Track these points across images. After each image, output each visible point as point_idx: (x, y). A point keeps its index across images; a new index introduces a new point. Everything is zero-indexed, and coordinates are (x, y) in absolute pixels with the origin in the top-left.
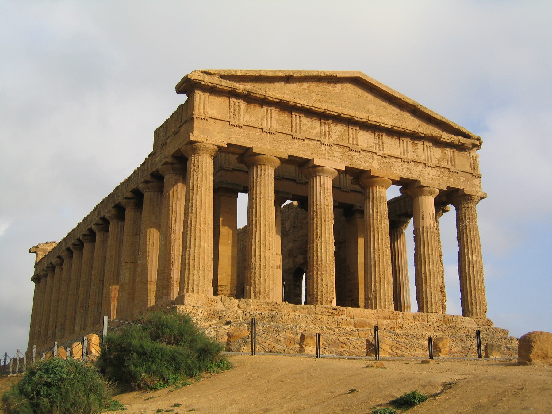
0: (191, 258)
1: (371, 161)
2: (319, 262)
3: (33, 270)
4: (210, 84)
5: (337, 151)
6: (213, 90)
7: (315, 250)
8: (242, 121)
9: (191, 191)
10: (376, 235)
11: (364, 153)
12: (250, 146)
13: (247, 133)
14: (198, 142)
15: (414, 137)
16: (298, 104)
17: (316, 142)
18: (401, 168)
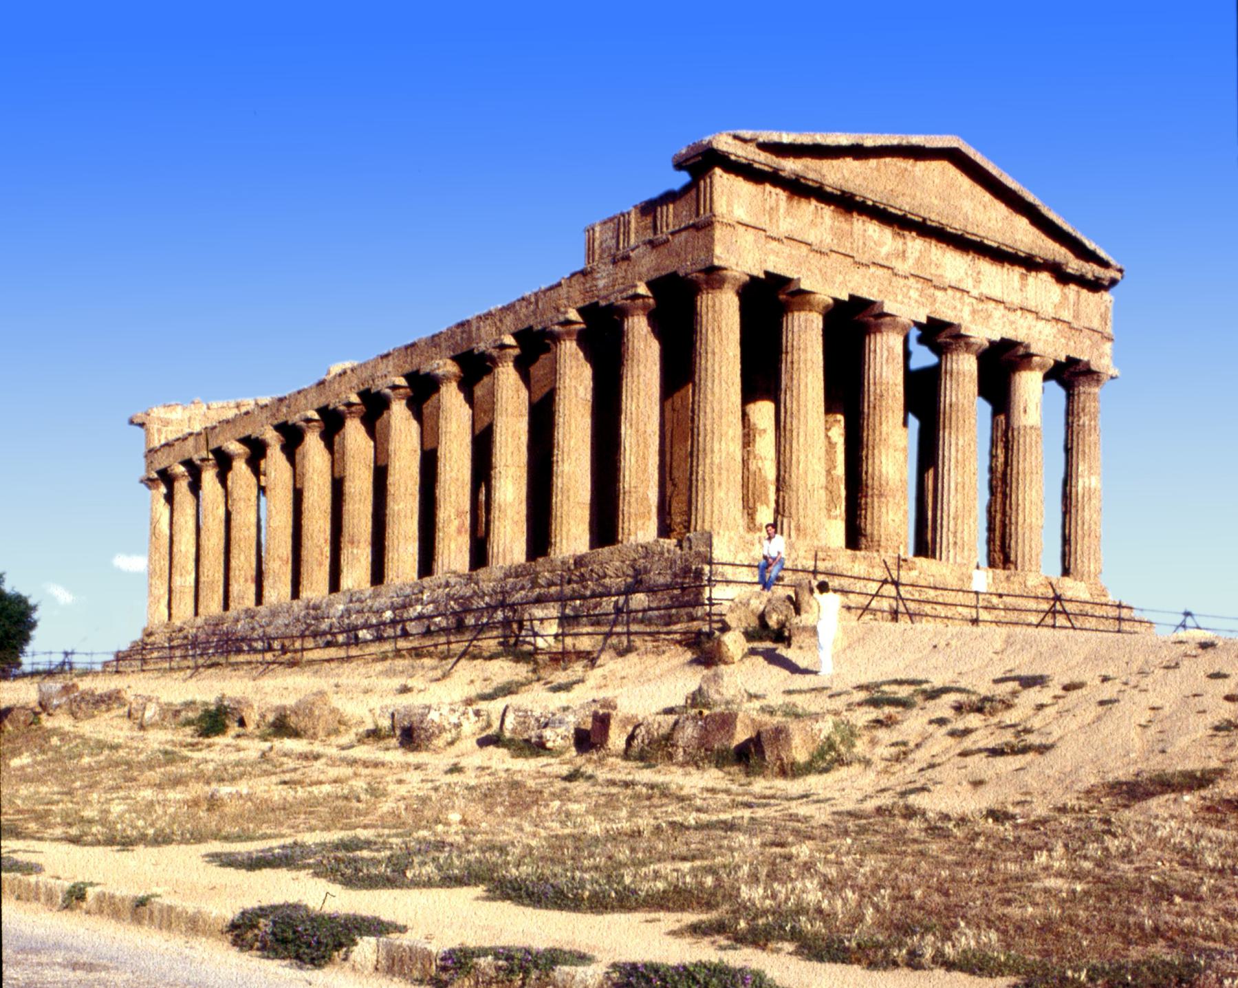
1: (959, 306)
8: (781, 229)
12: (795, 276)
14: (725, 269)
17: (886, 270)
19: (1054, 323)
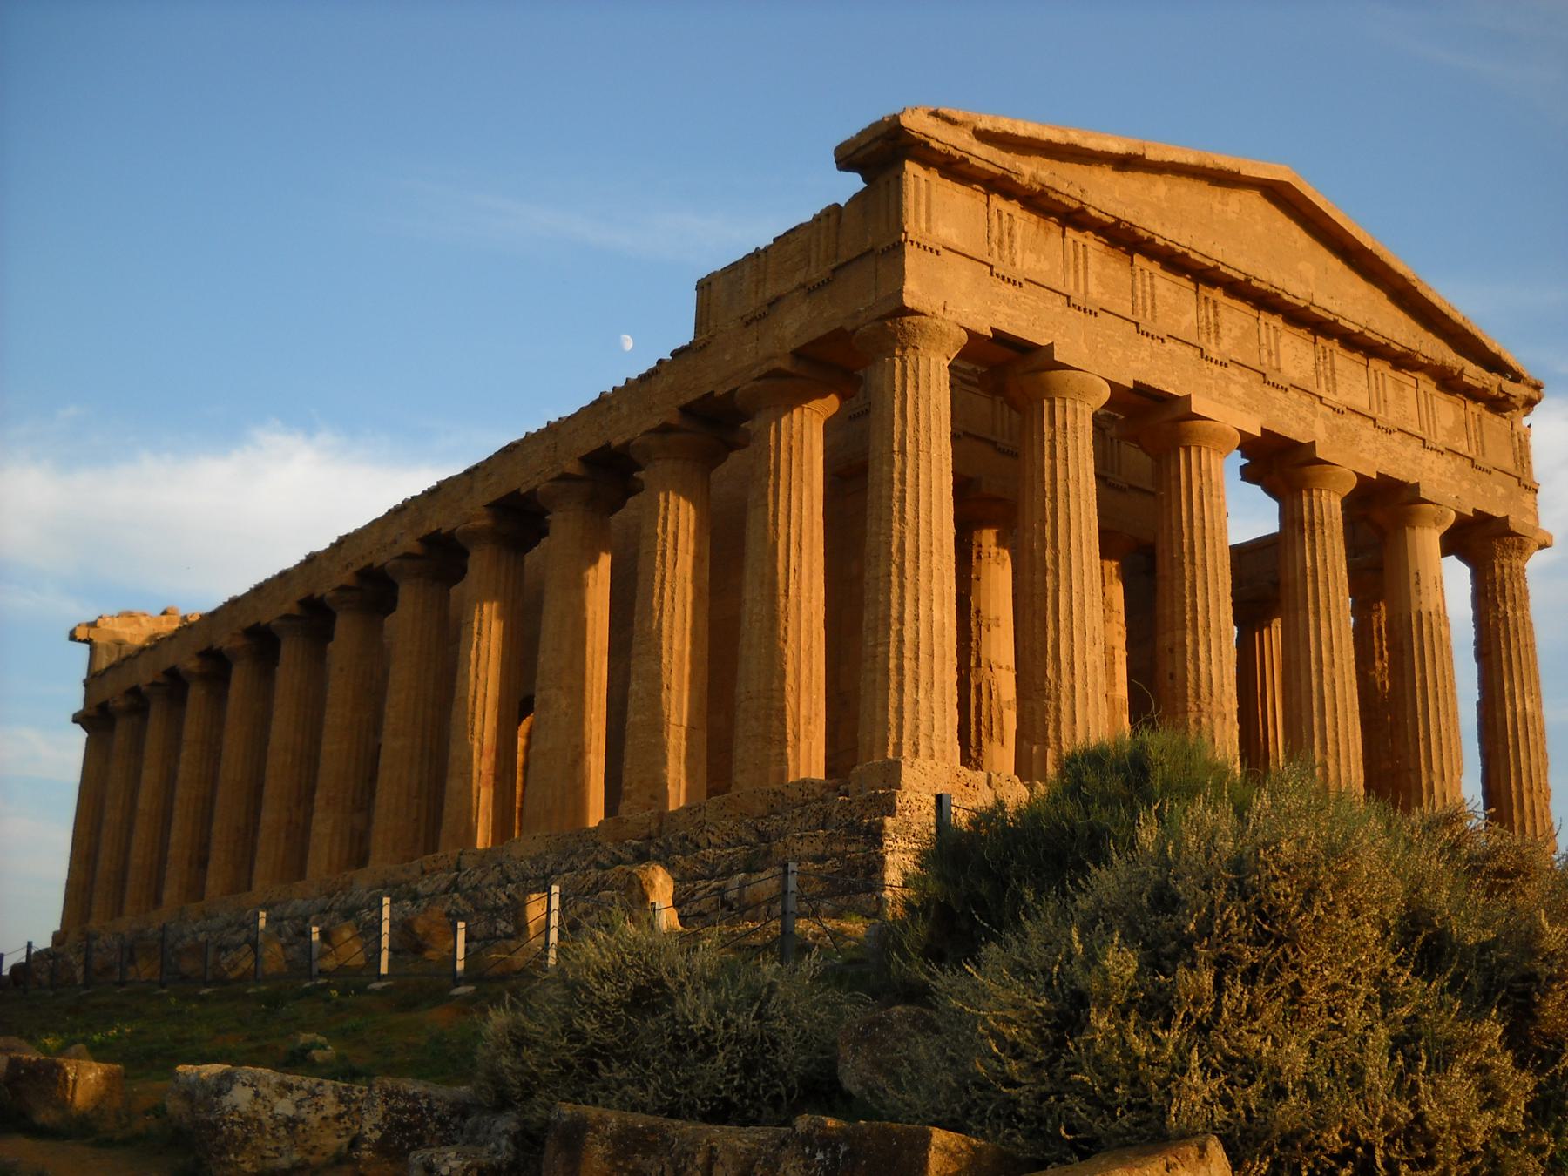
0: (908, 653)
1: (1310, 417)
2: (1204, 691)
3: (80, 692)
4: (952, 151)
5: (1236, 383)
6: (954, 168)
7: (1189, 656)
8: (1018, 266)
9: (897, 458)
10: (1323, 623)
11: (1296, 396)
12: (1044, 342)
13: (1034, 304)
14: (923, 314)
15: (1403, 361)
16: (1157, 238)
18: (1372, 446)
19: (1448, 457)
